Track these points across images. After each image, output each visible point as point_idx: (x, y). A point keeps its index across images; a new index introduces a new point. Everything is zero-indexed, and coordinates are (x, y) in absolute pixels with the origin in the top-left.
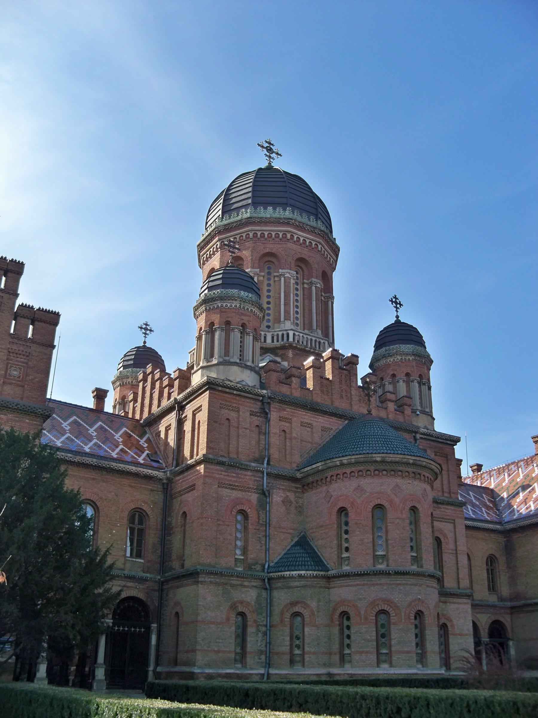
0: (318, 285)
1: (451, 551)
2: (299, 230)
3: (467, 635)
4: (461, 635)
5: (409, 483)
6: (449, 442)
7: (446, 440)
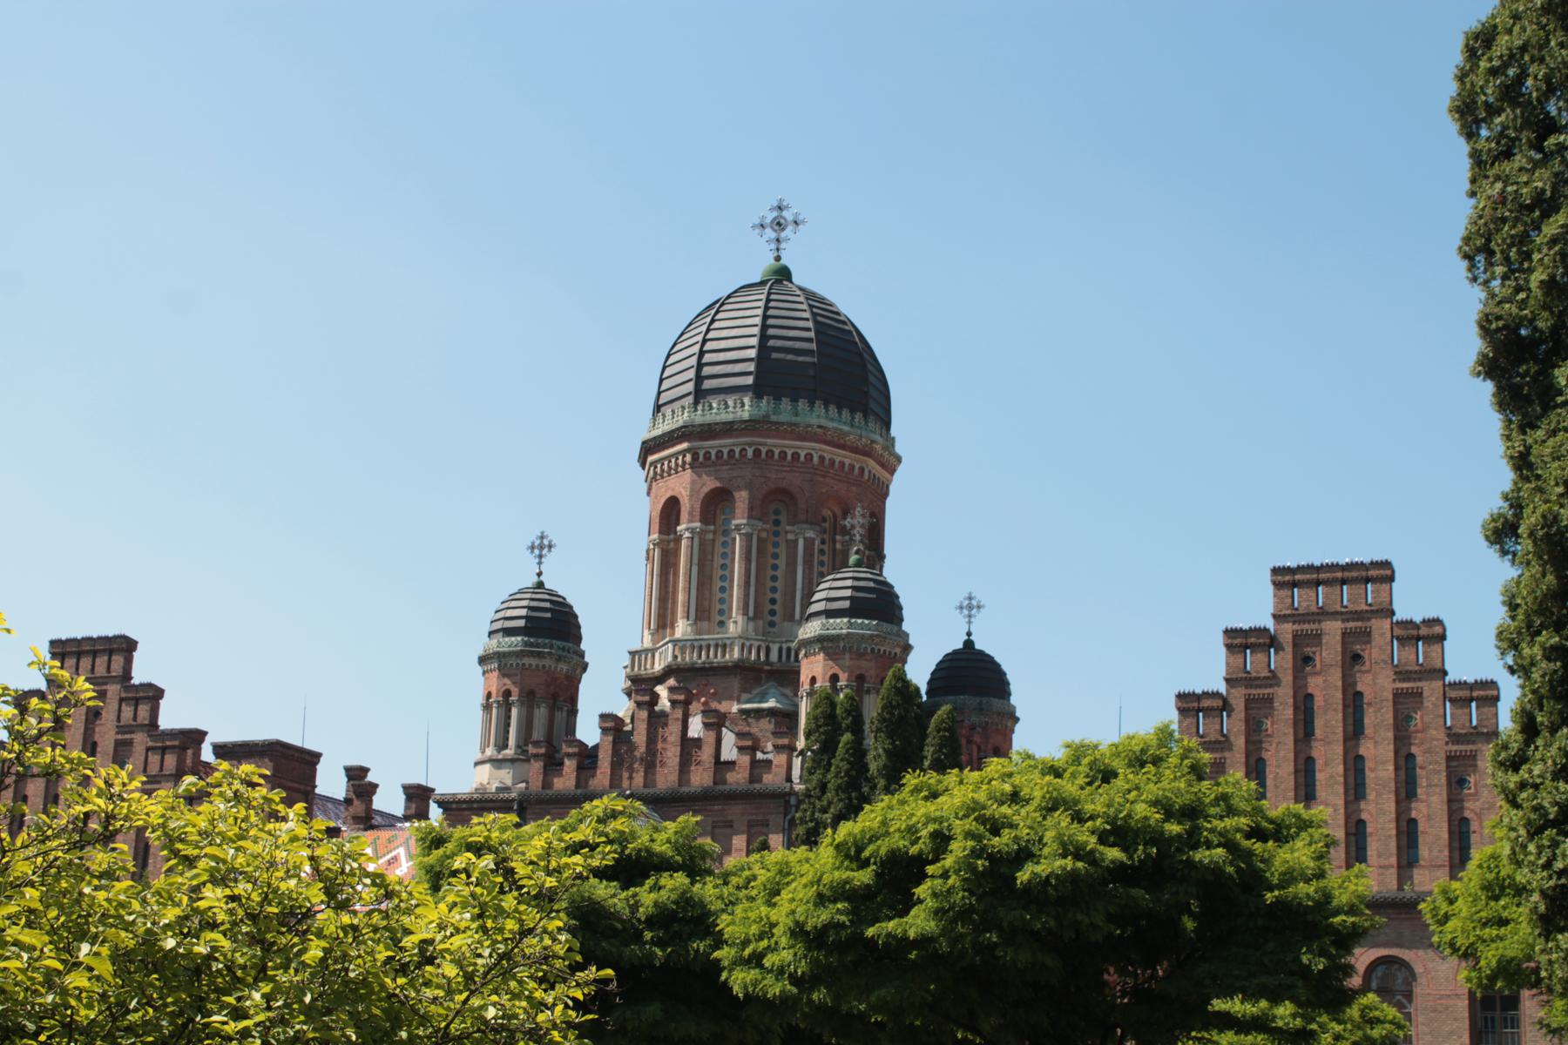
2: (706, 439)
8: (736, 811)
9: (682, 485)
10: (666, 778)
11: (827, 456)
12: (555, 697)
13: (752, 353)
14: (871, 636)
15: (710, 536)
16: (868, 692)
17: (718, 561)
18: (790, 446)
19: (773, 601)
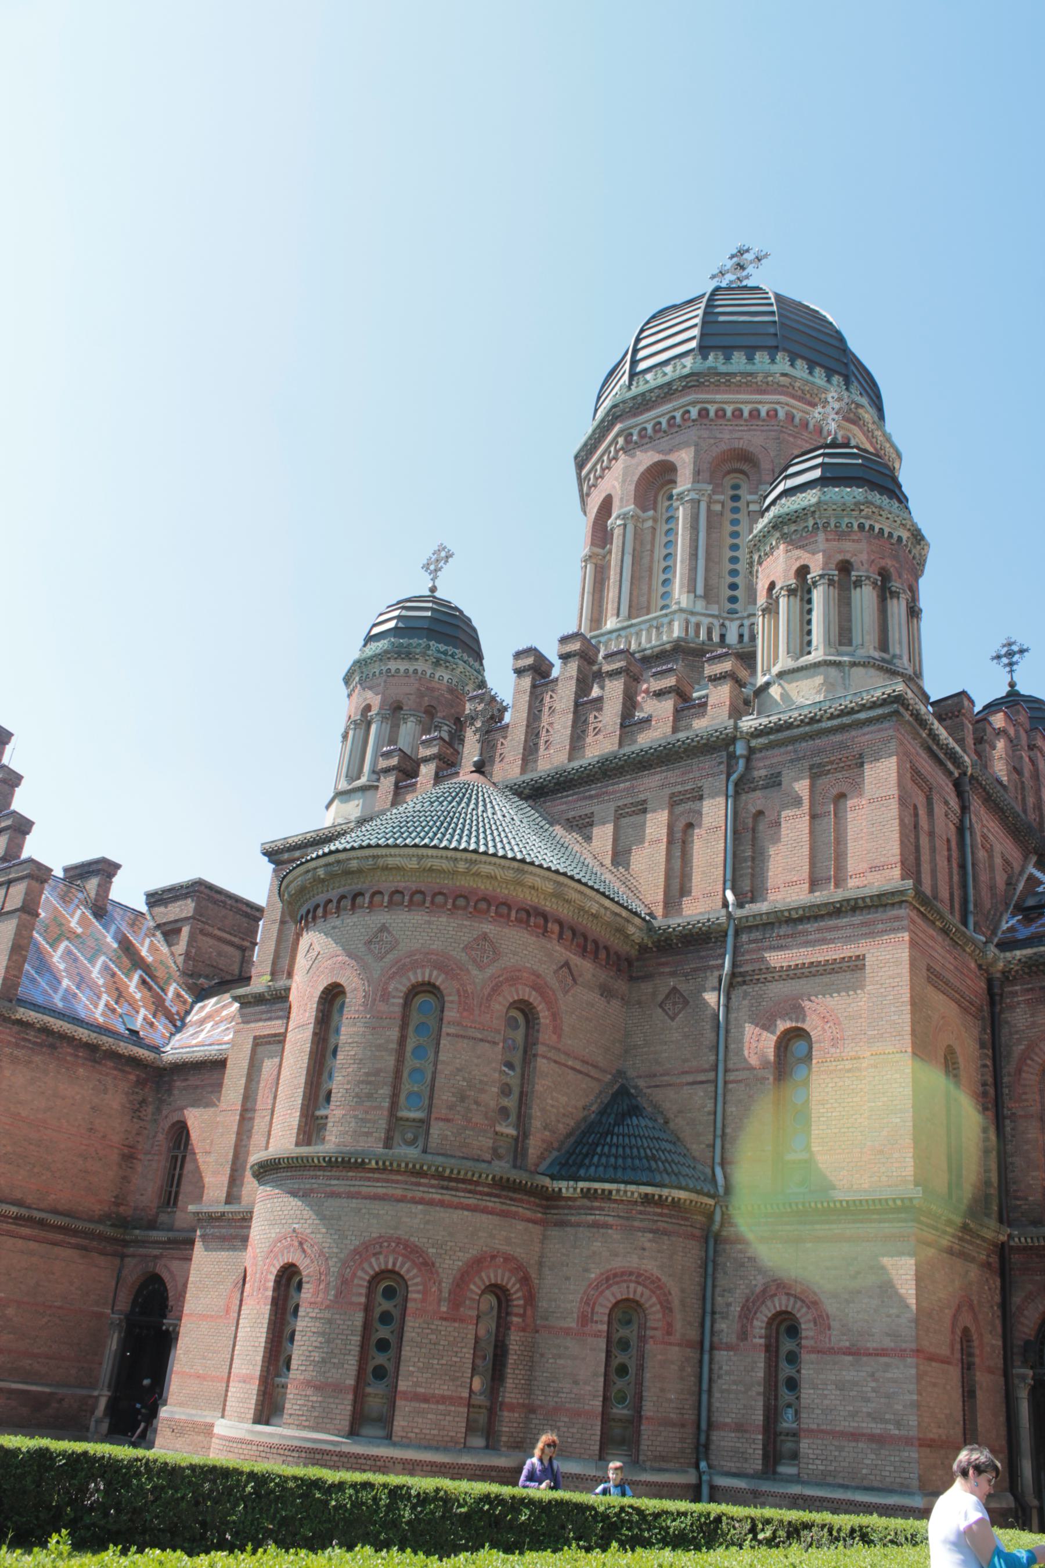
0: (693, 495)
1: (848, 1065)
2: (641, 413)
3: (882, 1352)
4: (855, 1352)
5: (334, 928)
6: (862, 716)
7: (843, 713)
8: (651, 784)
9: (618, 480)
10: (553, 758)
11: (798, 416)
12: (430, 712)
13: (695, 332)
14: (857, 504)
15: (650, 523)
16: (858, 584)
17: (660, 552)
18: (746, 401)
19: (733, 586)
